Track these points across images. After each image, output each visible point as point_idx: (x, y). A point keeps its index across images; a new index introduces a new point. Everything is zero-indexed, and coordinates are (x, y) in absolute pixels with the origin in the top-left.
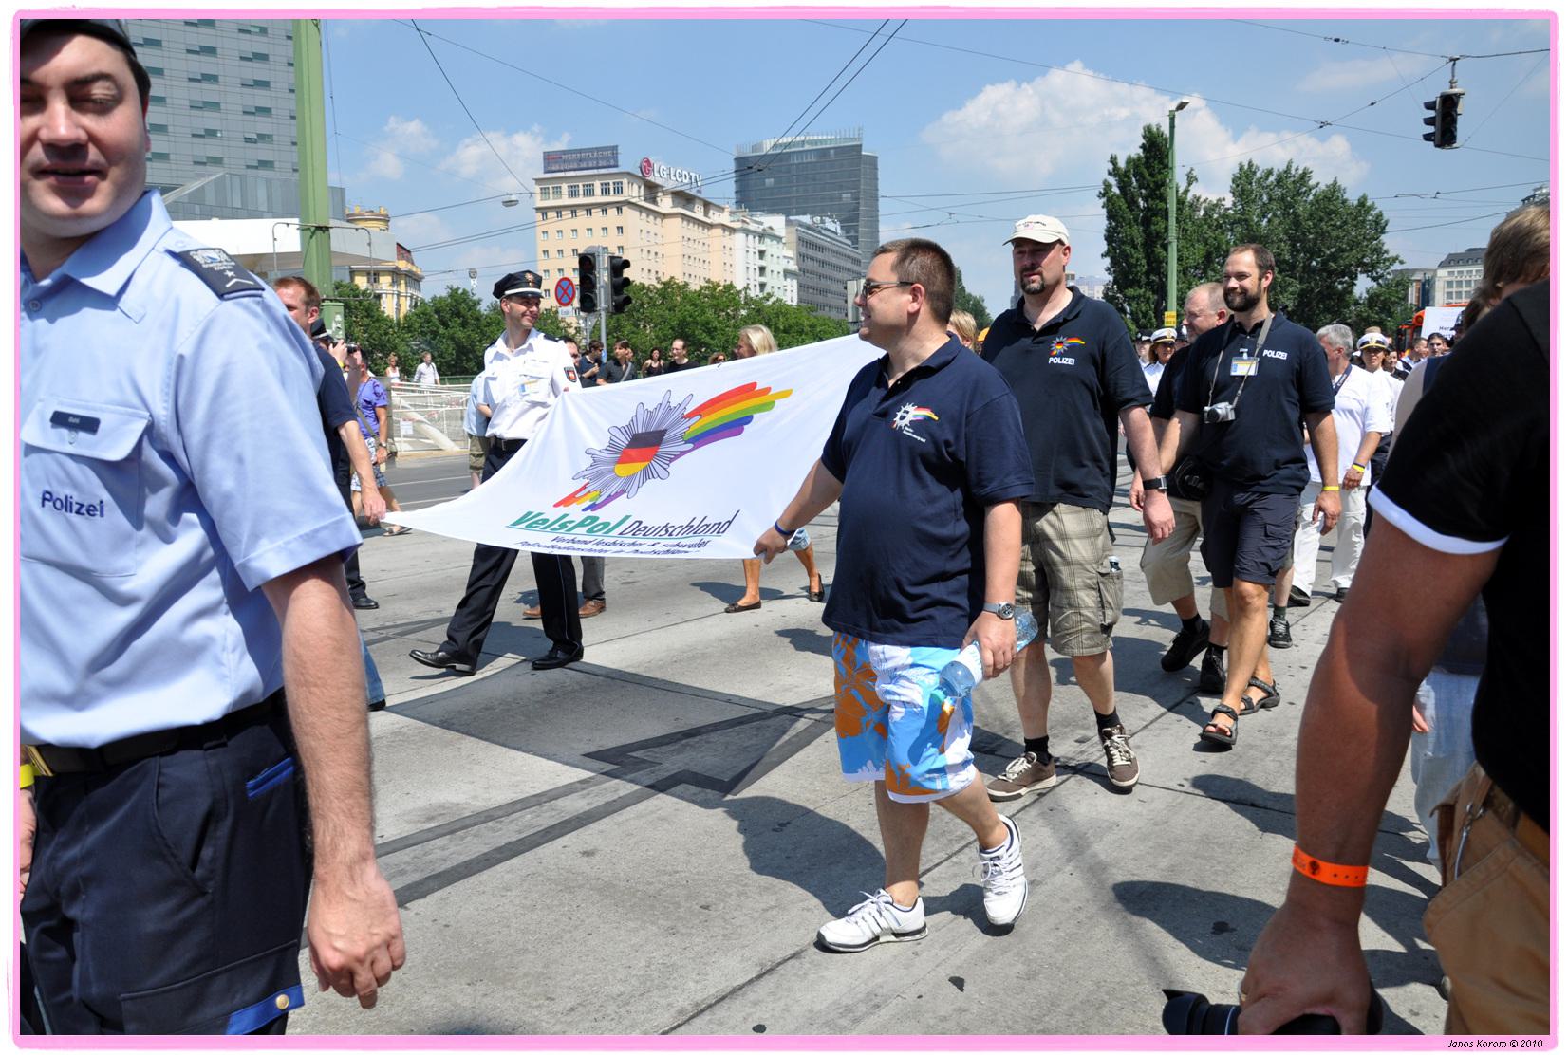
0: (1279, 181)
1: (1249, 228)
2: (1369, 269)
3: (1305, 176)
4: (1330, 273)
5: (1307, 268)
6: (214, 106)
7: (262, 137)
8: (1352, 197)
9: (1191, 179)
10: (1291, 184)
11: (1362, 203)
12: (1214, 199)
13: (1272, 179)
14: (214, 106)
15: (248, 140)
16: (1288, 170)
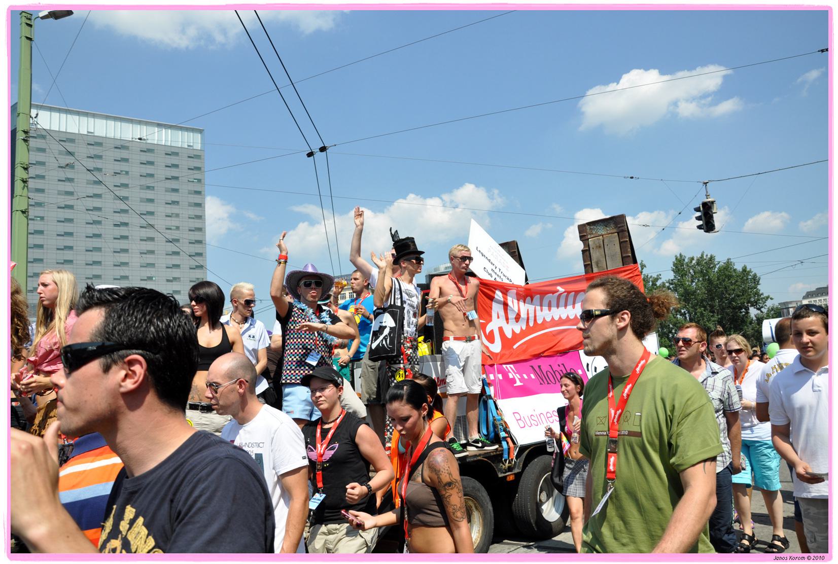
0: (698, 263)
1: (685, 289)
2: (755, 304)
3: (712, 258)
4: (734, 308)
5: (724, 309)
6: (152, 265)
7: (175, 279)
8: (739, 267)
9: (643, 266)
10: (705, 264)
11: (744, 270)
12: (655, 276)
13: (694, 262)
14: (152, 265)
15: (168, 281)
16: (702, 257)
